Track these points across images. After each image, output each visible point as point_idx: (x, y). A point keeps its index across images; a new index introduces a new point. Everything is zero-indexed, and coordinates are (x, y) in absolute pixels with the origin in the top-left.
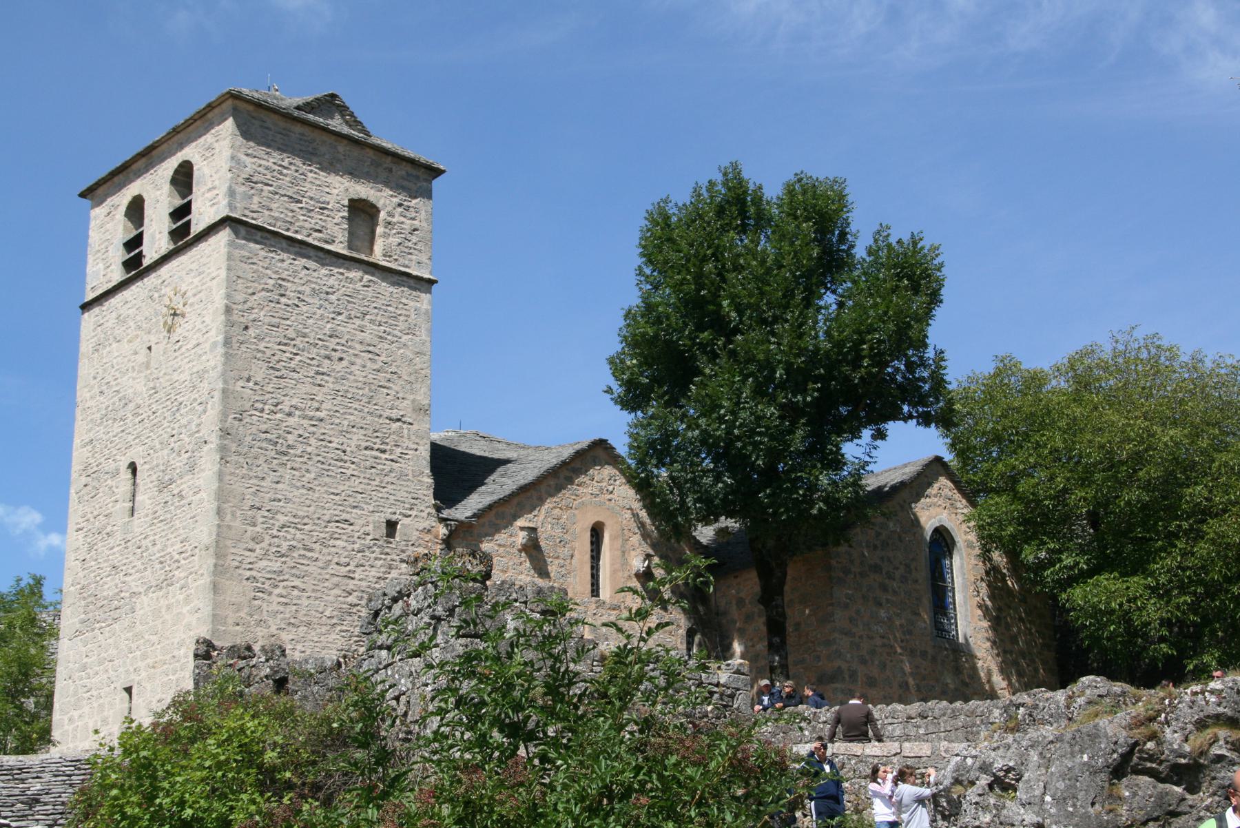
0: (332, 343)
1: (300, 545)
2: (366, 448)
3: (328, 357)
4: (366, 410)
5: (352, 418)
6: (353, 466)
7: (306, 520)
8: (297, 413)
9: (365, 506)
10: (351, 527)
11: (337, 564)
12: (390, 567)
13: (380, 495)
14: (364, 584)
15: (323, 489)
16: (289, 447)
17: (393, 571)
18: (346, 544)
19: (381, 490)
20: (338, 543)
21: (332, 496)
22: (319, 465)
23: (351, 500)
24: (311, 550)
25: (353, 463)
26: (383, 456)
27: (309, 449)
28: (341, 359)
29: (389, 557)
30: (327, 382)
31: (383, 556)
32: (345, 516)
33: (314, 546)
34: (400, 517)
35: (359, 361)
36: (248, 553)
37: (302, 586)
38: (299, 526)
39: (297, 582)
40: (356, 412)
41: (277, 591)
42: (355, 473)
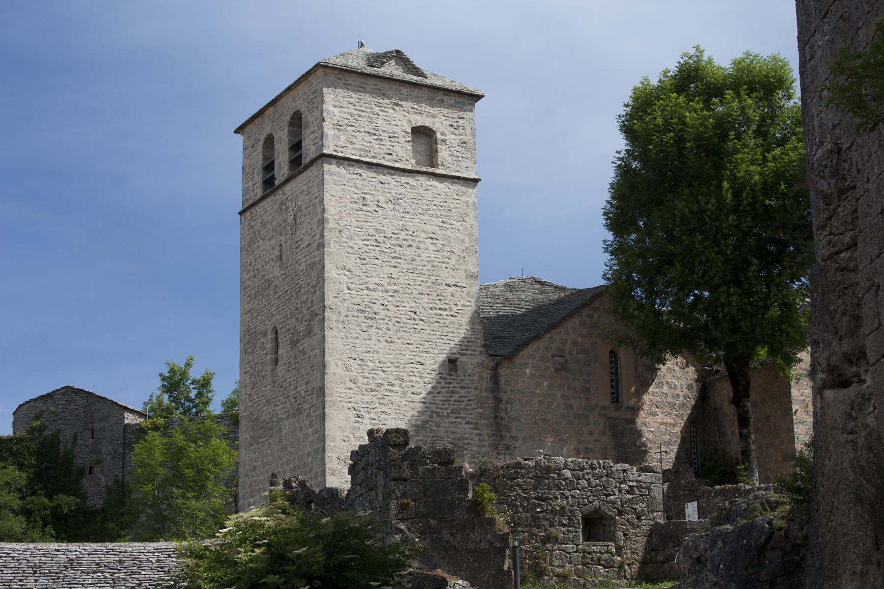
0: (403, 235)
2: (431, 309)
6: (421, 322)
7: (389, 364)
10: (423, 367)
13: (443, 342)
14: (434, 406)
19: (444, 337)
21: (407, 346)
24: (393, 385)
26: (444, 313)
27: (389, 314)
29: (451, 386)
31: (447, 385)
32: (418, 359)
34: (458, 356)
38: (384, 369)
40: (422, 283)
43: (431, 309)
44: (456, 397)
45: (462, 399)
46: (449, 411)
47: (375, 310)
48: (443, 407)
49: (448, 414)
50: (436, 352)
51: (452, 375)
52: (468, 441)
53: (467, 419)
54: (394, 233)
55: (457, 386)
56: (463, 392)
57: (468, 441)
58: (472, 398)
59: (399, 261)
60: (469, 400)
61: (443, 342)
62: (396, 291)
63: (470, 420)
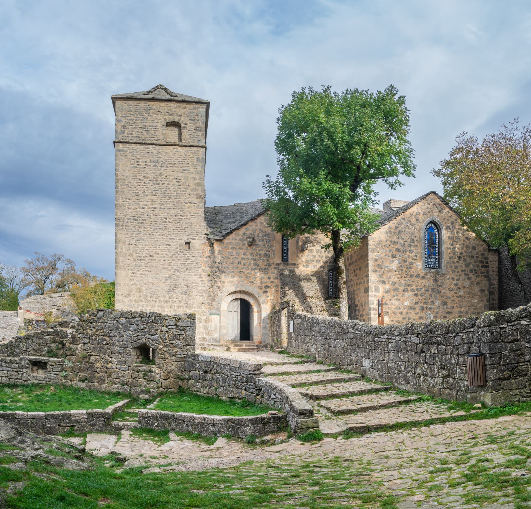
0: (160, 178)
1: (148, 256)
2: (176, 216)
3: (158, 184)
4: (175, 201)
8: (146, 207)
12: (187, 259)
14: (176, 267)
16: (143, 220)
20: (164, 253)
26: (183, 218)
27: (151, 220)
28: (163, 184)
32: (167, 243)
33: (154, 255)
34: (191, 240)
35: (171, 183)
36: (128, 261)
39: (147, 269)
41: (139, 273)
43: (176, 216)
44: (189, 262)
46: (185, 269)
53: (195, 273)
62: (155, 208)
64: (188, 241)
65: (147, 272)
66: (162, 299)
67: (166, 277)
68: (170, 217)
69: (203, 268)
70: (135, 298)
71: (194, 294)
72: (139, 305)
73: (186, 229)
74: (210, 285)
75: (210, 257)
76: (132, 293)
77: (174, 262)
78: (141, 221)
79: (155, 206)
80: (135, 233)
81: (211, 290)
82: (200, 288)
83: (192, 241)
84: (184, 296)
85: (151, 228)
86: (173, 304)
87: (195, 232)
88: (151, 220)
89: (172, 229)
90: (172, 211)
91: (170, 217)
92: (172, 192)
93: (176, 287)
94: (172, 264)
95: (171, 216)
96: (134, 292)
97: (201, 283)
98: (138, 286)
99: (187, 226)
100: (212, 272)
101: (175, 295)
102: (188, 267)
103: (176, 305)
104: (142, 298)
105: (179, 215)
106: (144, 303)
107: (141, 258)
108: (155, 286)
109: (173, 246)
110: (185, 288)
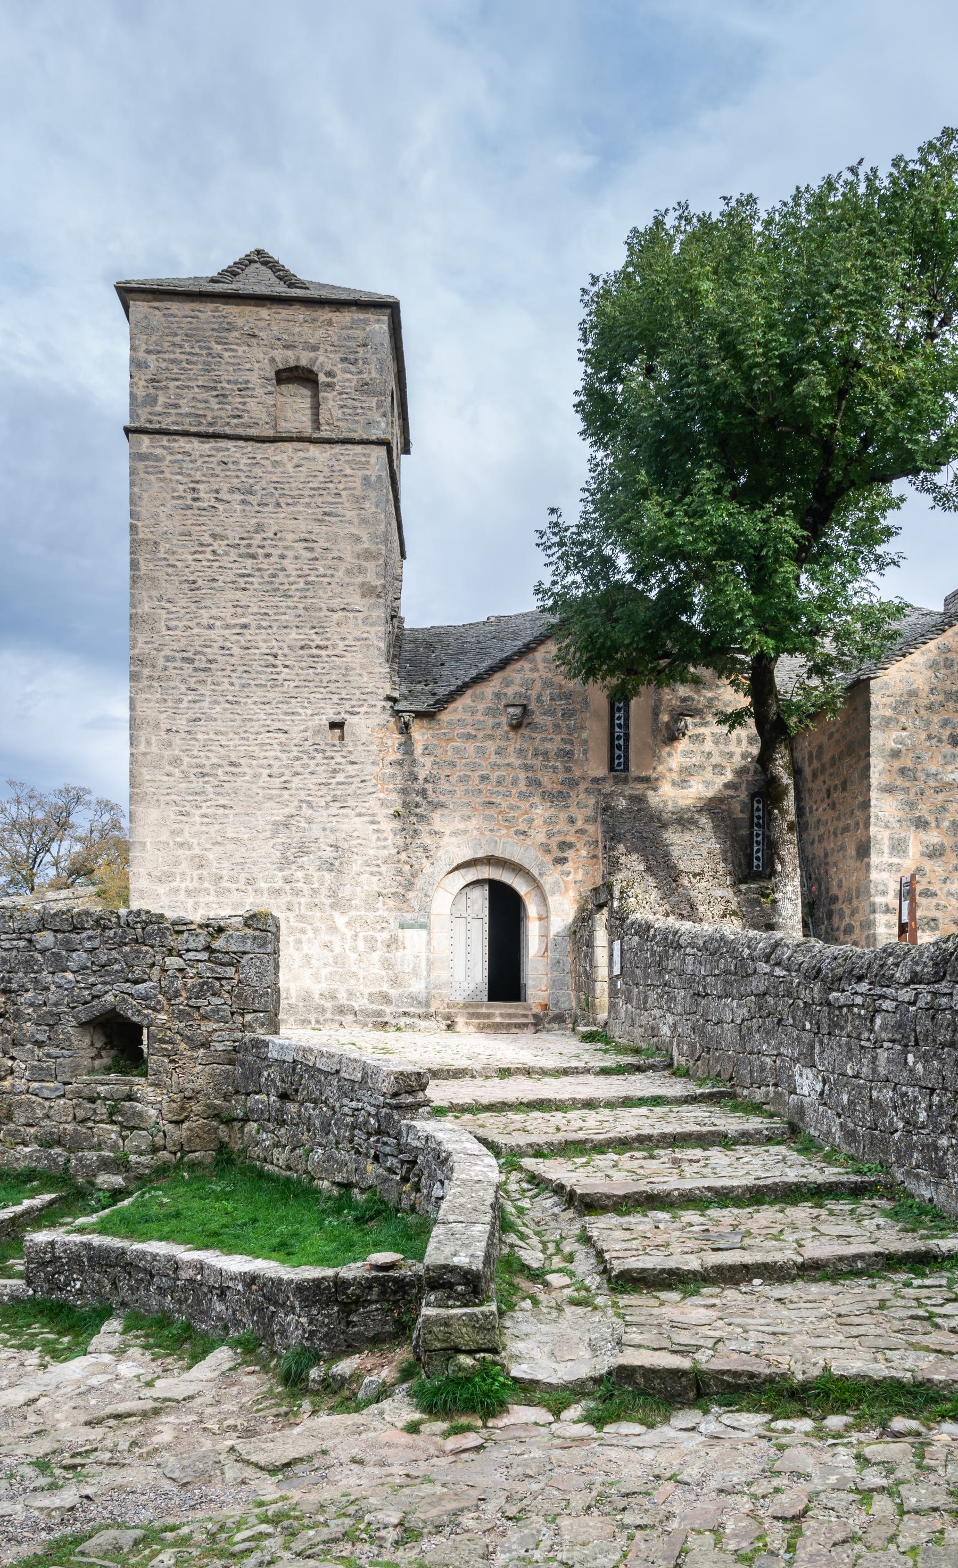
0: (257, 539)
1: (225, 763)
2: (302, 648)
3: (253, 556)
4: (301, 606)
5: (283, 617)
6: (286, 670)
9: (301, 711)
11: (270, 776)
13: (320, 696)
14: (303, 793)
15: (249, 701)
17: (338, 775)
18: (279, 754)
19: (322, 690)
20: (271, 754)
21: (262, 706)
22: (245, 675)
23: (285, 706)
25: (286, 666)
26: (323, 653)
27: (232, 660)
28: (268, 555)
29: (333, 762)
30: (252, 583)
31: (326, 761)
32: (277, 725)
33: (242, 761)
34: (347, 716)
37: (231, 803)
39: (222, 801)
40: (288, 611)
42: (288, 677)
43: (302, 648)
44: (340, 777)
45: (350, 780)
46: (329, 799)
47: (210, 657)
48: (320, 793)
49: (327, 803)
50: (309, 712)
51: (334, 745)
52: (360, 841)
53: (358, 810)
54: (242, 539)
55: (343, 760)
56: (351, 769)
57: (360, 841)
58: (367, 778)
59: (250, 579)
60: (363, 781)
61: (320, 696)
62: (245, 626)
63: (364, 810)
64: (337, 719)
65: (221, 811)
66: (263, 885)
67: (275, 824)
68: (286, 651)
69: (382, 795)
70: (187, 883)
71: (356, 867)
72: (197, 903)
73: (332, 685)
74: (401, 842)
75: (400, 763)
76: (178, 870)
77: (296, 779)
78: (203, 665)
79: (243, 620)
80: (186, 699)
81: (403, 856)
82: (372, 852)
83: (350, 720)
84: (328, 876)
85: (232, 684)
86: (295, 900)
87: (357, 692)
88: (232, 660)
89: (292, 684)
90: (293, 634)
91: (286, 651)
92: (292, 579)
93: (303, 850)
94: (293, 785)
95: (290, 647)
96: (184, 866)
97: (374, 837)
98: (197, 850)
99: (334, 677)
100: (405, 804)
101: (300, 874)
102: (339, 793)
103: (303, 900)
104: (206, 885)
105: (313, 644)
106: (212, 898)
107: (205, 771)
108: (243, 849)
109: (296, 734)
110: (329, 853)
